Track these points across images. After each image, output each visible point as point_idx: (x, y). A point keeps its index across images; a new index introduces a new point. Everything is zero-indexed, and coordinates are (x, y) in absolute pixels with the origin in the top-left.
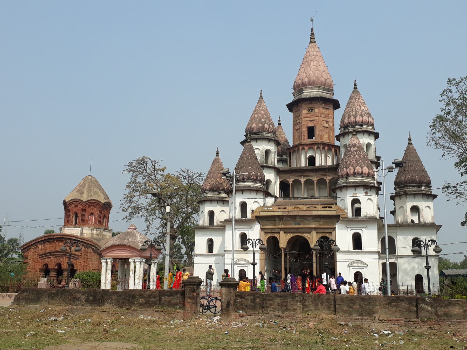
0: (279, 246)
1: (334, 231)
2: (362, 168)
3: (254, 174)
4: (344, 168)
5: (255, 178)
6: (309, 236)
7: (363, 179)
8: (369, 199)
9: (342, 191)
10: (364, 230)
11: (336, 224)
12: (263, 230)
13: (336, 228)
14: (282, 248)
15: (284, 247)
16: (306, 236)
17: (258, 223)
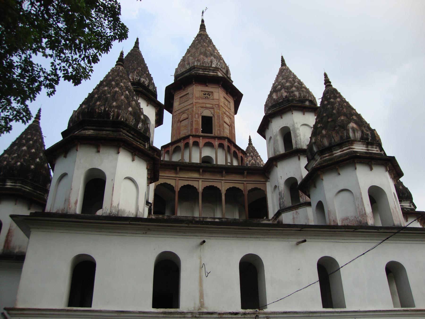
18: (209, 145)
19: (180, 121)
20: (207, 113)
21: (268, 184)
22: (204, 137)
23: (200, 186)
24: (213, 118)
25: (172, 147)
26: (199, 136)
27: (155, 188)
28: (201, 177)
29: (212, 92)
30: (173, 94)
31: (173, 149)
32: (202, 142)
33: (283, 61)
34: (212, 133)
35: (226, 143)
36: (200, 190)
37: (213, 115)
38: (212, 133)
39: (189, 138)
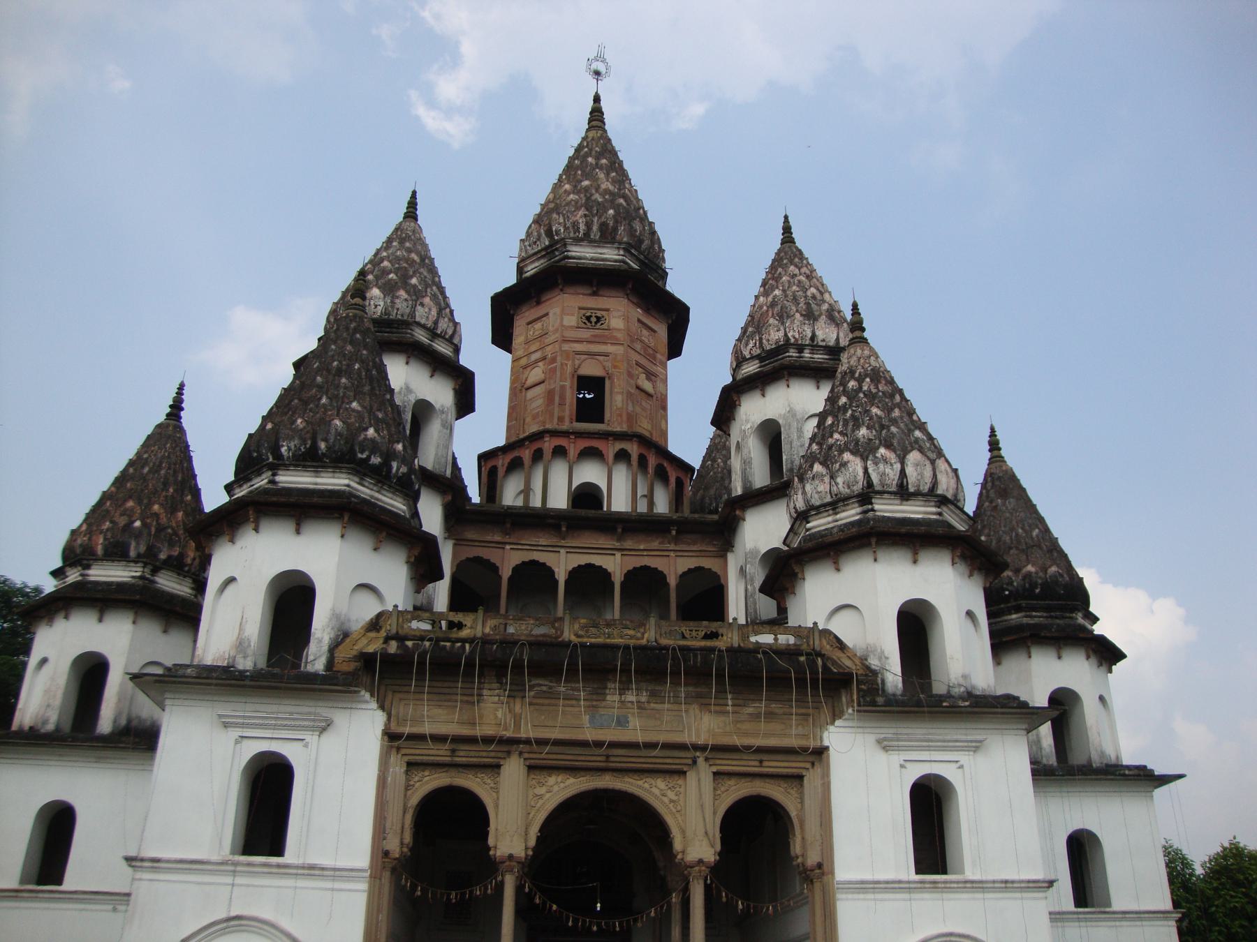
0: (489, 849)
1: (818, 770)
2: (933, 462)
3: (373, 440)
4: (847, 456)
5: (376, 460)
6: (671, 795)
7: (940, 514)
8: (970, 614)
9: (841, 566)
10: (964, 758)
11: (823, 727)
12: (398, 749)
13: (827, 748)
14: (511, 857)
15: (523, 855)
16: (653, 791)
17: (374, 705)
18: (590, 454)
19: (526, 386)
20: (591, 369)
21: (730, 556)
22: (580, 435)
23: (562, 564)
24: (607, 383)
25: (503, 459)
26: (565, 434)
27: (454, 570)
28: (563, 543)
29: (607, 310)
30: (512, 312)
31: (506, 465)
32: (573, 449)
33: (787, 229)
34: (601, 421)
35: (633, 449)
36: (561, 577)
37: (608, 374)
38: (601, 421)
39: (543, 437)
